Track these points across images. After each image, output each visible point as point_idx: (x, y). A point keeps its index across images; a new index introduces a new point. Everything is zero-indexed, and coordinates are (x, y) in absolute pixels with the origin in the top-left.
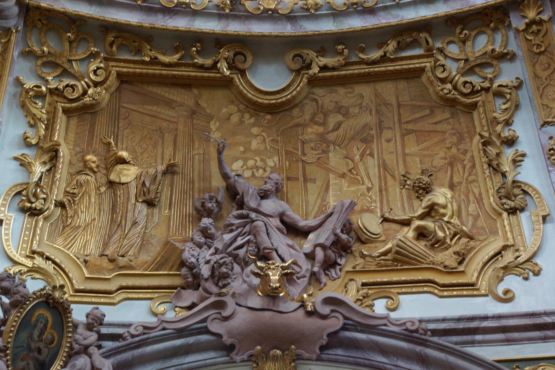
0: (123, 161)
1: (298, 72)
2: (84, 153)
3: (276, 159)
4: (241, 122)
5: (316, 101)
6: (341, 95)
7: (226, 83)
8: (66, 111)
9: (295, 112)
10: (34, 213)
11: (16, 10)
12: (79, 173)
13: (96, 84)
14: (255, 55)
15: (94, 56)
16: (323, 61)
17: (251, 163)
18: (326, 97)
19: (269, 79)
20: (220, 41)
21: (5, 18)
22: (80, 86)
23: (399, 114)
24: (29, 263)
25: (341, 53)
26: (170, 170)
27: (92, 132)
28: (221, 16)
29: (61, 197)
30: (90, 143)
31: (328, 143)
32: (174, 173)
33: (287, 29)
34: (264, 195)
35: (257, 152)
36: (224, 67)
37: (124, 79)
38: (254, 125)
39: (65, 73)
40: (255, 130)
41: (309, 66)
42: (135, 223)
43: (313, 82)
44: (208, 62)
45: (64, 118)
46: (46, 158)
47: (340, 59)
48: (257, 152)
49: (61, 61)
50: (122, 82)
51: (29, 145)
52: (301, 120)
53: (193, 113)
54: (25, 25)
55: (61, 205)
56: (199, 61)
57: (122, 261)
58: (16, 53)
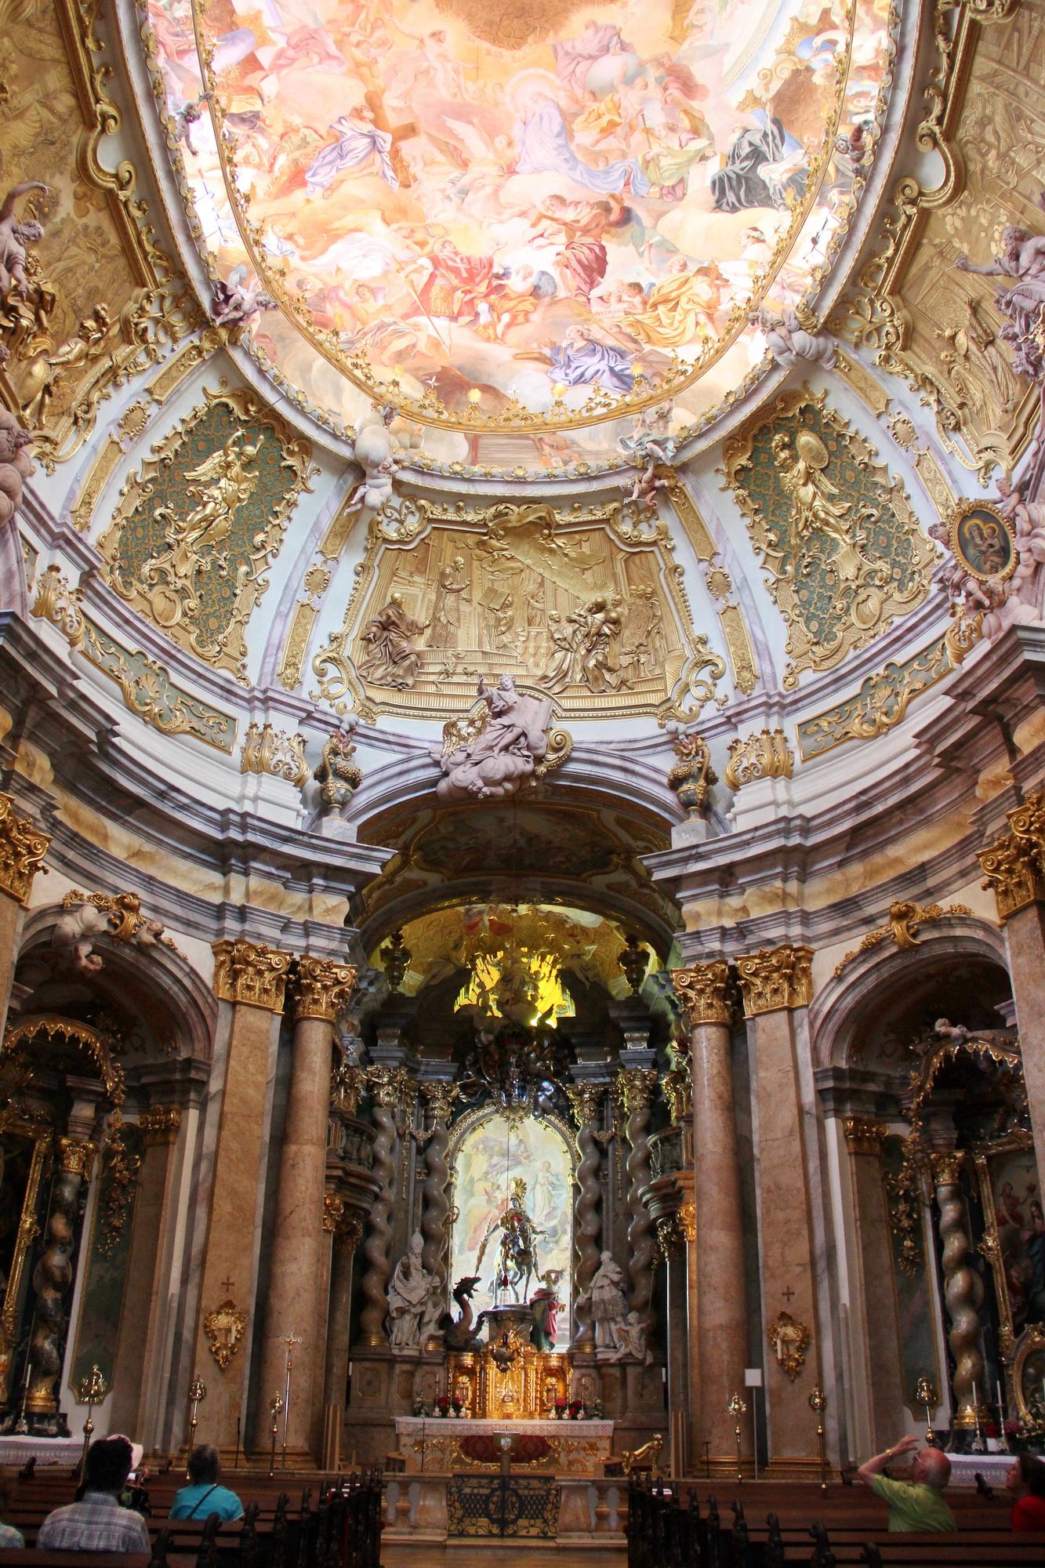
0: (953, 337)
1: (936, 144)
2: (938, 357)
3: (1002, 211)
4: (963, 219)
5: (968, 142)
6: (971, 115)
7: (925, 215)
8: (903, 349)
9: (971, 167)
10: (957, 428)
11: (821, 340)
12: (949, 372)
13: (892, 314)
14: (911, 175)
15: (872, 302)
16: (933, 116)
17: (997, 236)
18: (967, 131)
19: (935, 171)
20: (888, 198)
21: (825, 350)
22: (888, 328)
23: (1008, 67)
24: (981, 464)
25: (932, 98)
26: (975, 307)
27: (926, 340)
28: (867, 190)
29: (959, 400)
30: (934, 349)
31: (1006, 154)
32: (979, 303)
33: (894, 138)
34: (1015, 256)
35: (991, 223)
36: (912, 210)
37: (896, 290)
38: (969, 210)
39: (878, 330)
40: (973, 212)
41: (932, 135)
42: (995, 369)
43: (949, 136)
44: (903, 219)
45: (909, 352)
46: (928, 388)
47: (938, 101)
48: (991, 223)
49: (869, 328)
50: (899, 293)
51: (918, 390)
52: (979, 166)
53: (941, 253)
54: (836, 336)
55: (962, 406)
56: (899, 225)
57: (1010, 406)
58: (854, 356)
